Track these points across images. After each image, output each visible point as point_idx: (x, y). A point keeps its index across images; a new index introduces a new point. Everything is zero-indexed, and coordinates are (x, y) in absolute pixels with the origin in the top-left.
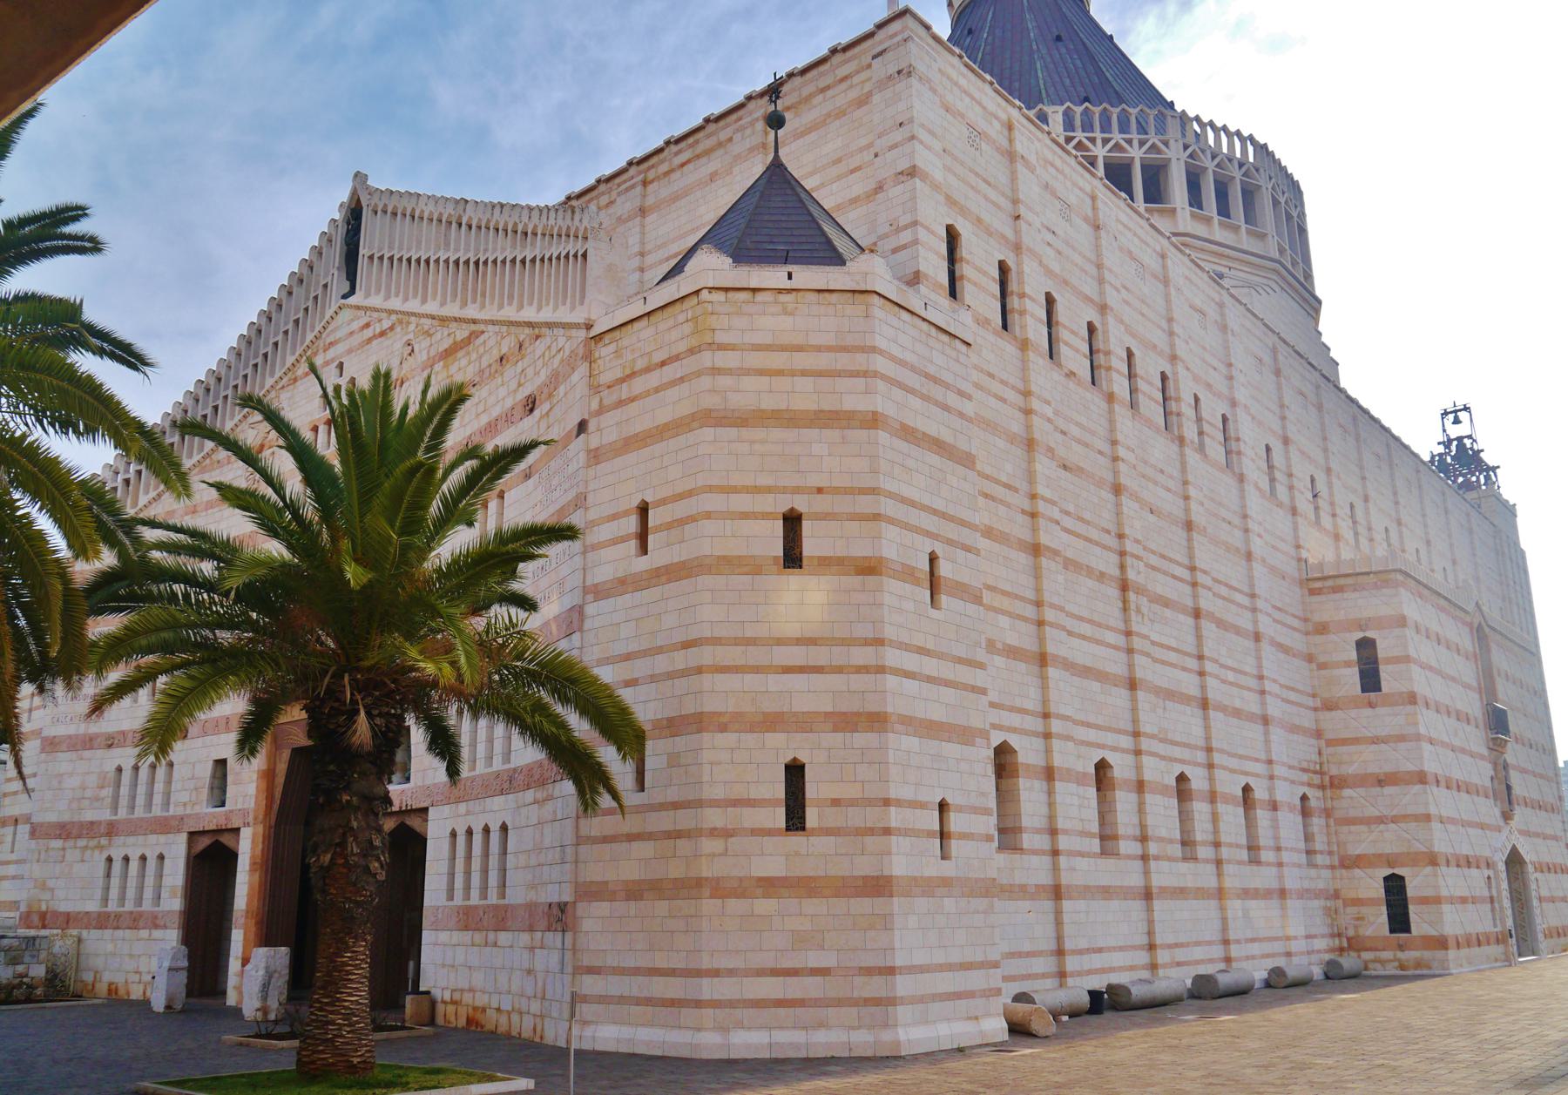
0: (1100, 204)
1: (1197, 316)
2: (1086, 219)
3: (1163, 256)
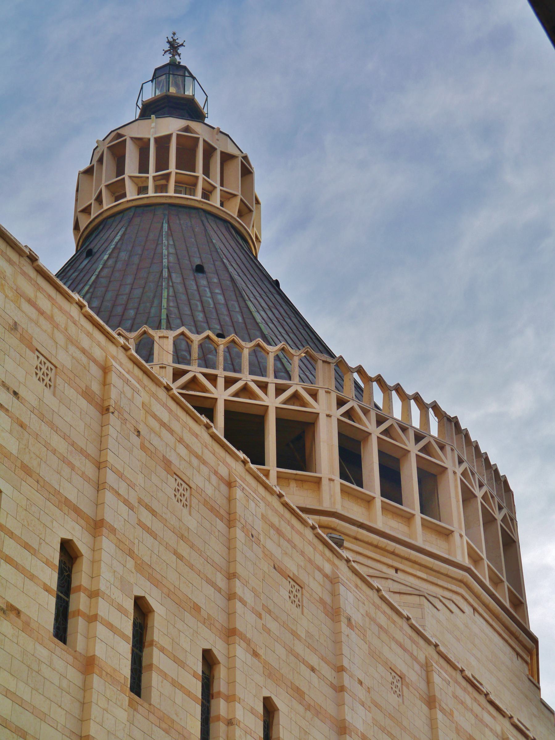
0: (114, 378)
1: (286, 586)
2: (87, 394)
3: (230, 484)
